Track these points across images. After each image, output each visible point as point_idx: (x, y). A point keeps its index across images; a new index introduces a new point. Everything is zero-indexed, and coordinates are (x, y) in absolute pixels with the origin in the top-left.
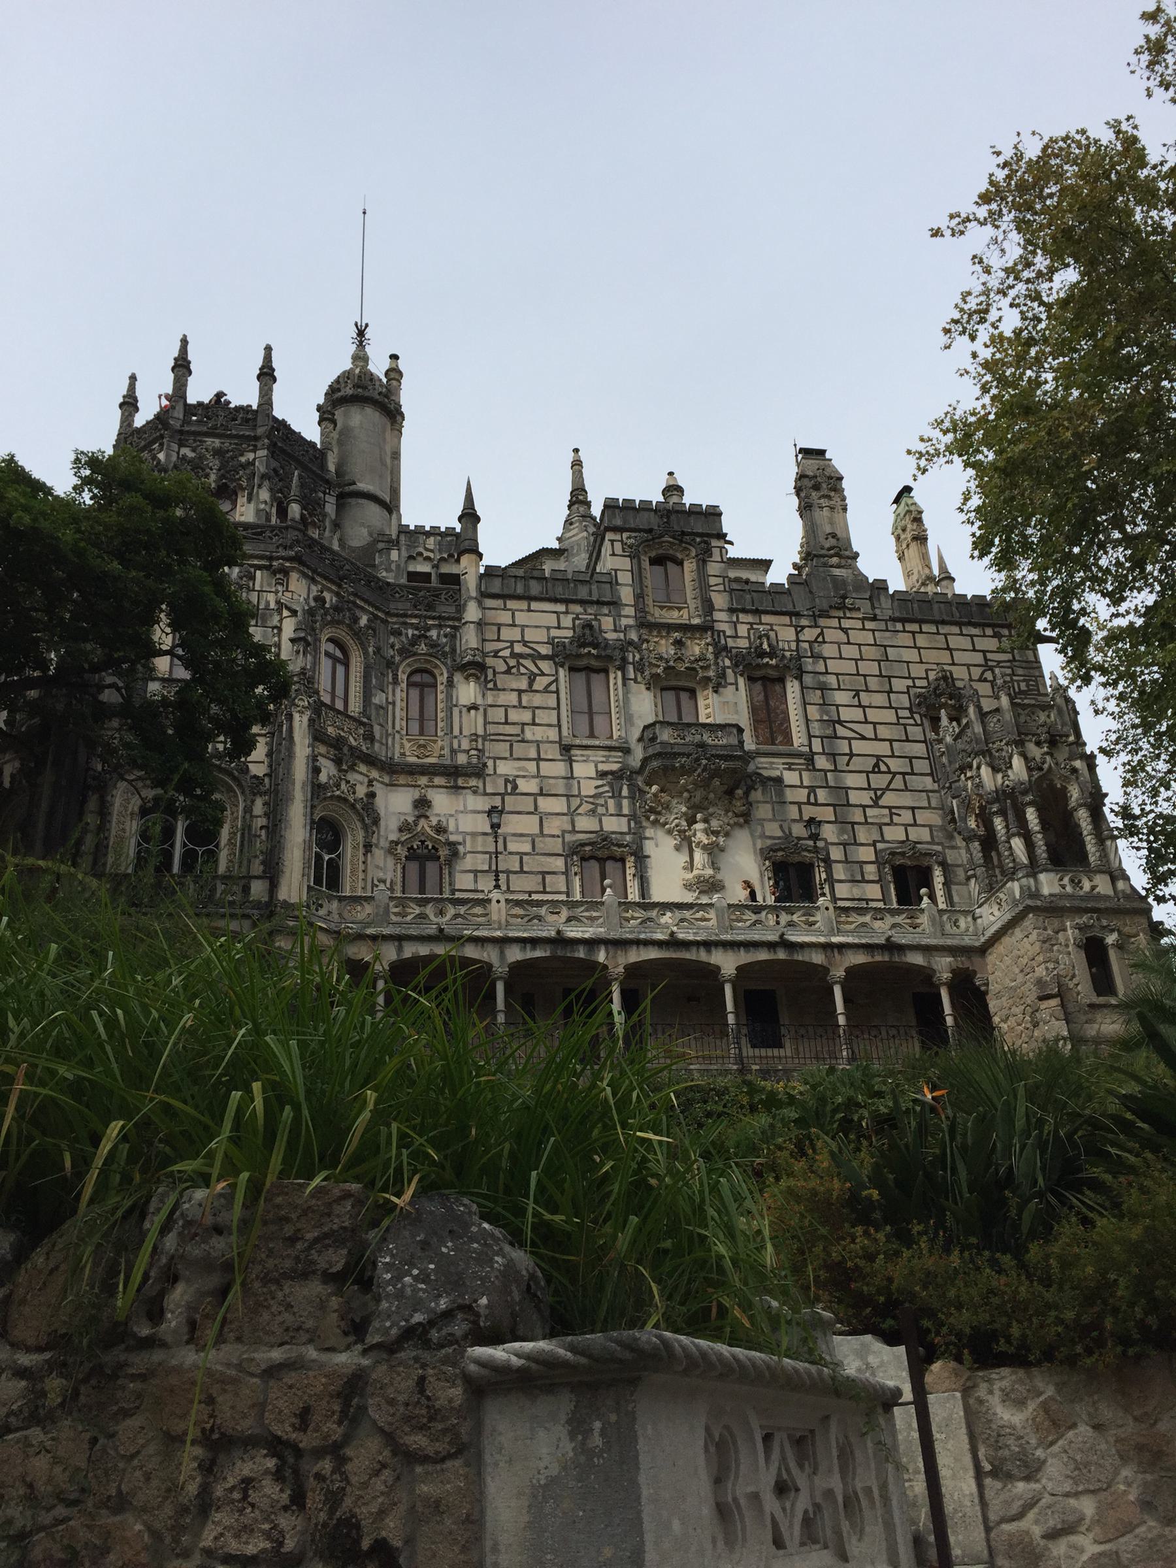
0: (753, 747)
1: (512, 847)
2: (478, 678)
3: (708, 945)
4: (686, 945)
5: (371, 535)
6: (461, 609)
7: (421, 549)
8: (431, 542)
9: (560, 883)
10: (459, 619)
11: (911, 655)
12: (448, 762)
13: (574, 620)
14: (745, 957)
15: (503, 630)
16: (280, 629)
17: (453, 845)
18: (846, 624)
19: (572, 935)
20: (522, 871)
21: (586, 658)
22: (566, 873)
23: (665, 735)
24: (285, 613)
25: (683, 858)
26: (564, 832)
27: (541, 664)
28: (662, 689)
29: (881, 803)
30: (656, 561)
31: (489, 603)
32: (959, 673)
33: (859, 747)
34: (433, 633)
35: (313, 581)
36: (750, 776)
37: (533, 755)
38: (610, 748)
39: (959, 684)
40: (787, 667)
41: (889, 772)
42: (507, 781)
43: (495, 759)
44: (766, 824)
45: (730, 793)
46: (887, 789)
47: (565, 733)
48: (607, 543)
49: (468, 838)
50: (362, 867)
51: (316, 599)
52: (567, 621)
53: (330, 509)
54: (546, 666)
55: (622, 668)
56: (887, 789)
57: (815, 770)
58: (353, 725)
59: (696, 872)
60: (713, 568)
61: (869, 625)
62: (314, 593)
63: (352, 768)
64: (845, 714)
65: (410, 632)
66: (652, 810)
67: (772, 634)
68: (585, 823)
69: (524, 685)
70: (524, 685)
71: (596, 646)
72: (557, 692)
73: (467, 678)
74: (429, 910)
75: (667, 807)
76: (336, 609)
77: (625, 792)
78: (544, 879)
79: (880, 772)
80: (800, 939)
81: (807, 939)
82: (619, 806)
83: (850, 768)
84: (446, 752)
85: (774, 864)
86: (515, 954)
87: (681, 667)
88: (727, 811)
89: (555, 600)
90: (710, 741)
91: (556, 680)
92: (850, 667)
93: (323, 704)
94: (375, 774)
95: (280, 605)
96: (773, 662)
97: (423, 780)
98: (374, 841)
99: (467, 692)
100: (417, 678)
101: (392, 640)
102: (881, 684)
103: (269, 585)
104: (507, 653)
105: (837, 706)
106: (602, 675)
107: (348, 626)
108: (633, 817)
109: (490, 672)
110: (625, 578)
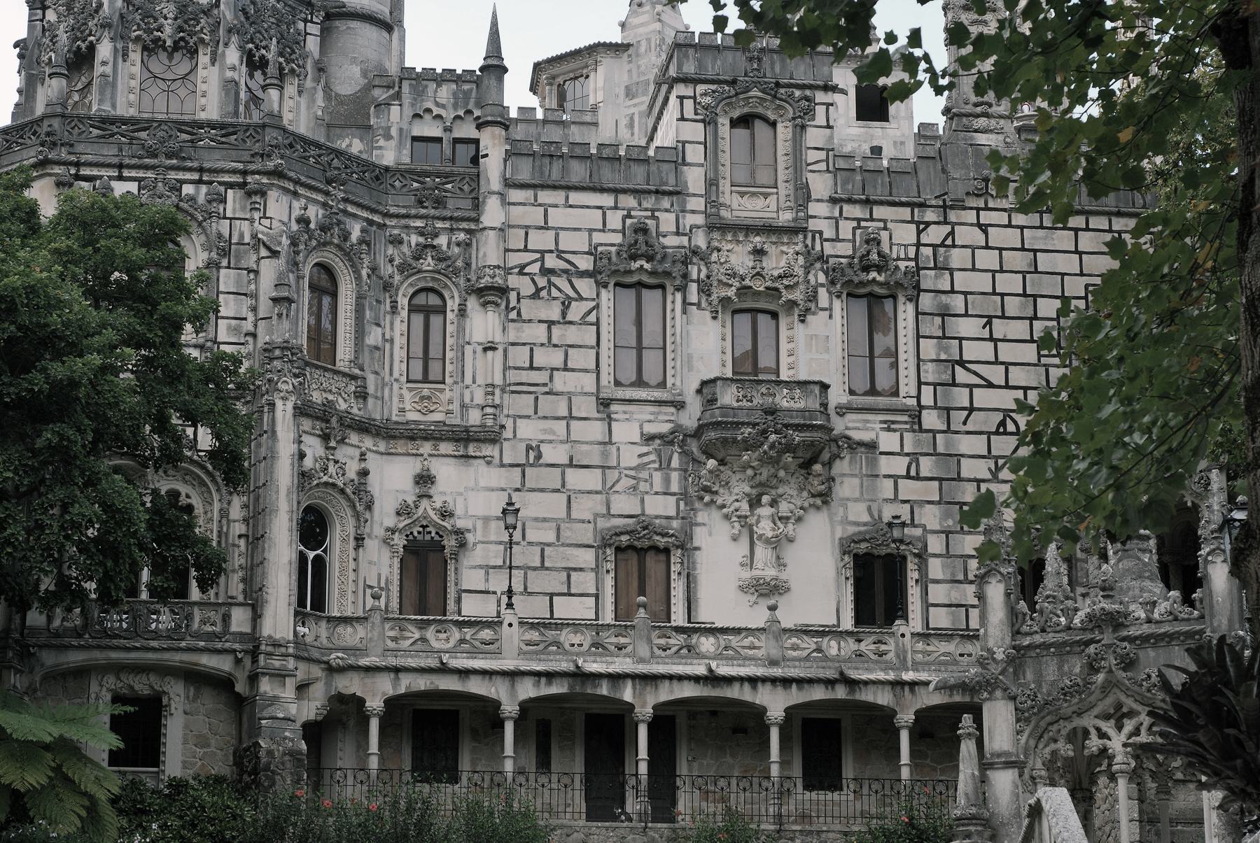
0: (844, 399)
1: (532, 535)
2: (497, 305)
3: (753, 681)
4: (729, 680)
5: (364, 74)
6: (477, 205)
7: (430, 105)
8: (445, 93)
9: (584, 582)
10: (476, 220)
11: (1069, 264)
12: (457, 421)
13: (624, 223)
14: (796, 696)
15: (533, 234)
16: (256, 272)
17: (459, 532)
18: (986, 217)
19: (593, 667)
20: (543, 567)
21: (640, 270)
22: (596, 569)
23: (728, 396)
24: (264, 252)
25: (743, 548)
26: (596, 515)
27: (576, 282)
28: (735, 312)
30: (744, 122)
31: (516, 195)
33: (983, 398)
34: (442, 241)
35: (295, 194)
36: (835, 441)
37: (566, 413)
38: (660, 403)
40: (899, 284)
41: (1017, 433)
42: (529, 448)
43: (516, 417)
44: (850, 504)
45: (807, 465)
47: (604, 382)
48: (673, 100)
49: (479, 524)
50: (352, 565)
51: (299, 221)
52: (615, 220)
53: (312, 44)
54: (586, 287)
55: (683, 289)
57: (921, 430)
58: (341, 382)
59: (756, 573)
60: (814, 136)
61: (1019, 219)
62: (296, 213)
63: (342, 441)
64: (972, 351)
65: (415, 239)
66: (707, 490)
67: (884, 235)
68: (624, 504)
69: (555, 314)
70: (554, 313)
71: (650, 259)
72: (597, 324)
73: (484, 305)
74: (430, 633)
76: (324, 228)
77: (675, 462)
78: (569, 577)
79: (1005, 433)
80: (864, 677)
81: (872, 677)
82: (667, 481)
83: (969, 427)
84: (455, 407)
85: (856, 556)
86: (528, 690)
87: (759, 286)
88: (801, 490)
89: (602, 190)
90: (785, 404)
91: (597, 307)
92: (982, 282)
93: (307, 364)
94: (368, 442)
95: (257, 242)
97: (426, 448)
98: (367, 530)
99: (484, 323)
100: (421, 300)
101: (390, 250)
102: (1023, 306)
103: (243, 209)
104: (534, 269)
105: (961, 339)
106: (659, 292)
107: (338, 246)
108: (684, 496)
109: (513, 296)
110: (695, 154)
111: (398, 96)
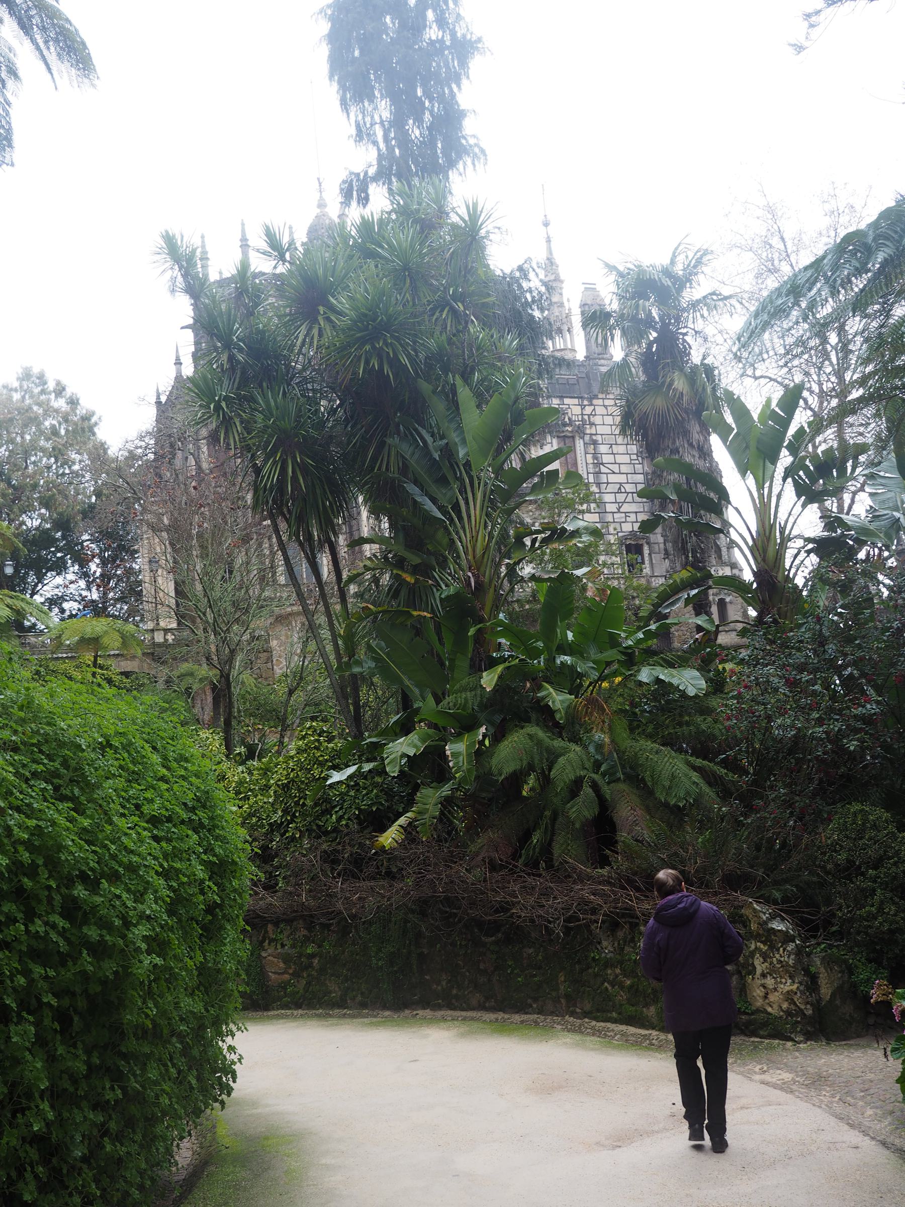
18: (607, 402)
29: (621, 510)
33: (612, 478)
46: (624, 502)
56: (624, 502)
64: (606, 459)
83: (607, 491)
96: (570, 429)
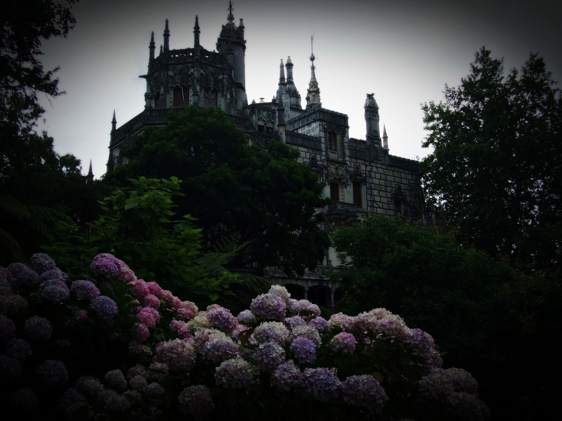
32: (403, 187)
39: (403, 191)
55: (322, 176)
61: (383, 167)
75: (335, 230)
86: (310, 284)
111: (254, 113)
